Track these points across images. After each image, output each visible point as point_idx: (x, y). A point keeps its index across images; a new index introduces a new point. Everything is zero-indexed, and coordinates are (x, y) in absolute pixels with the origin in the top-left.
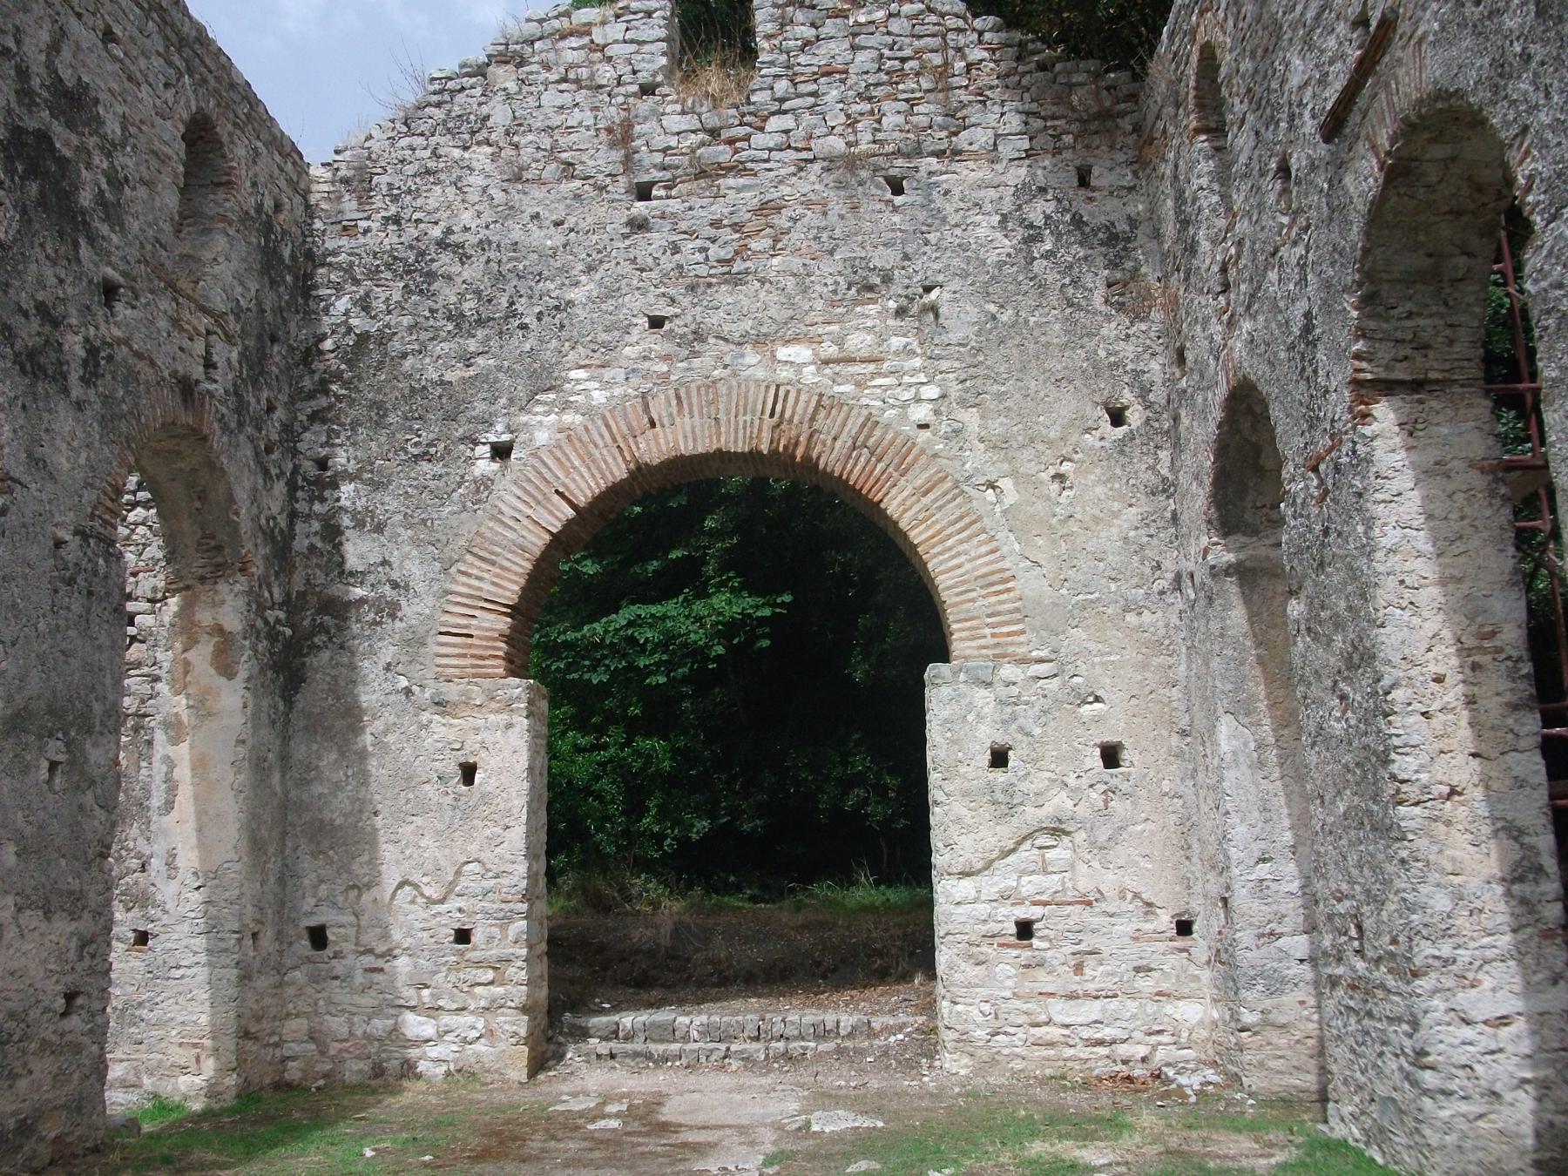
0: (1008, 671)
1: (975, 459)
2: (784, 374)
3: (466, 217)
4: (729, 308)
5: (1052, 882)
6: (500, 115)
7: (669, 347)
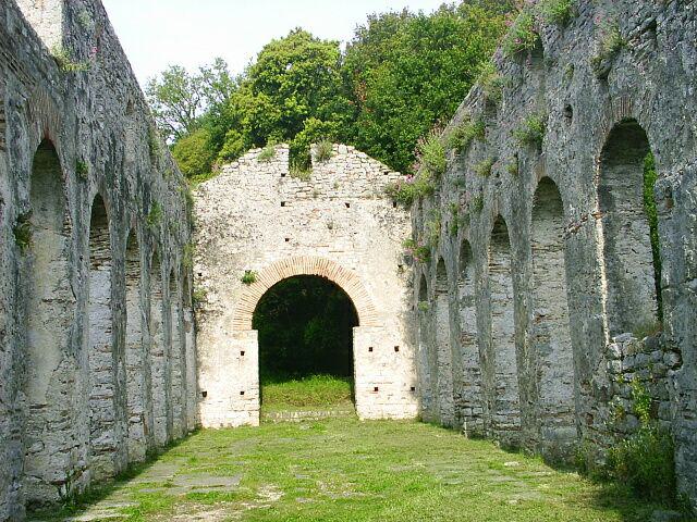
0: (373, 329)
1: (366, 277)
2: (320, 255)
3: (236, 209)
4: (305, 237)
5: (381, 379)
6: (244, 181)
7: (290, 247)
